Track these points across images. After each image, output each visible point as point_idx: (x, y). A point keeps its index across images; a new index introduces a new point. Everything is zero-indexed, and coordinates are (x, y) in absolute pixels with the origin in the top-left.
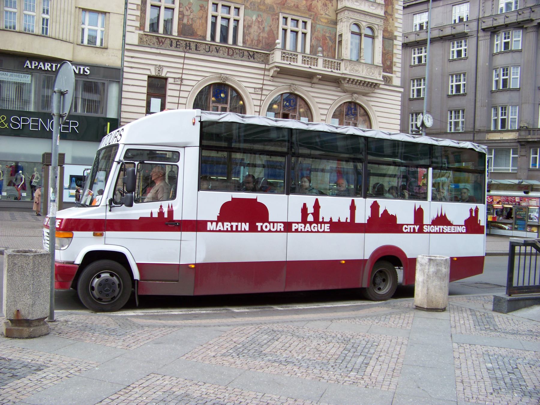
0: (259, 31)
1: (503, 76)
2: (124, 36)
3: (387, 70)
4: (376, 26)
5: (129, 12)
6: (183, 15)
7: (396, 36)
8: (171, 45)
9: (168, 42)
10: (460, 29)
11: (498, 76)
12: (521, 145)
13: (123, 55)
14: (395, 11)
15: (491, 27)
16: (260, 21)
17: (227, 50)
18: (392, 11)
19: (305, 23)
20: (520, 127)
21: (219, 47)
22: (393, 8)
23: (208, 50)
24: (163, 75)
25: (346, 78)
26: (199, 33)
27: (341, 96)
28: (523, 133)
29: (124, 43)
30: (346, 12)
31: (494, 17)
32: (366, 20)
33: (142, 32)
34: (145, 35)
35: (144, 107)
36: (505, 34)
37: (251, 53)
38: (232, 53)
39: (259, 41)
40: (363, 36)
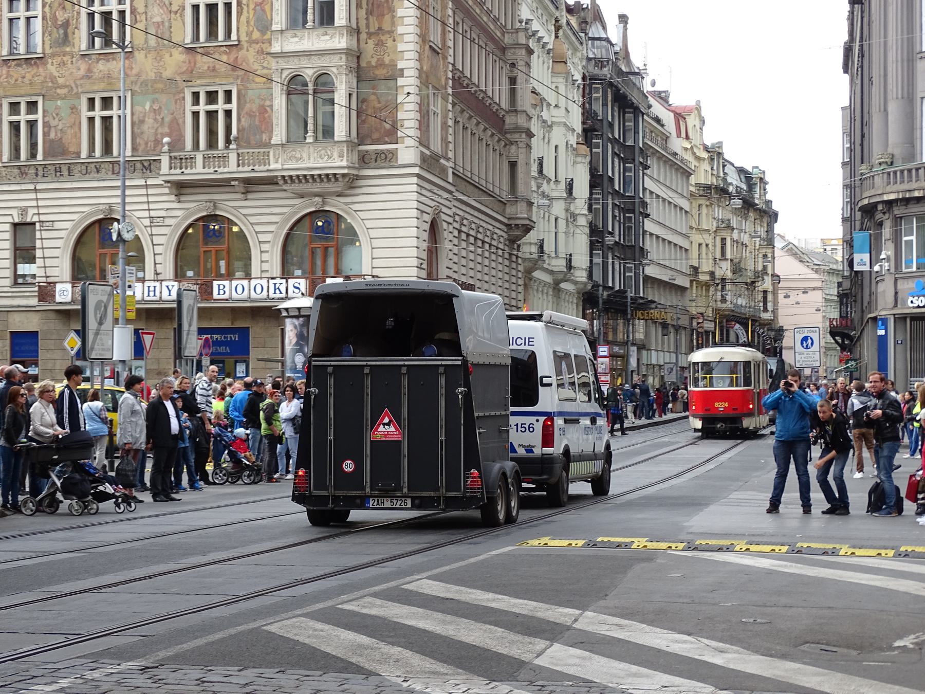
0: (156, 126)
3: (387, 139)
6: (50, 127)
7: (402, 70)
8: (37, 175)
16: (157, 108)
17: (111, 165)
18: (393, 24)
19: (228, 94)
22: (393, 17)
23: (84, 172)
24: (28, 220)
32: (311, 66)
34: (4, 167)
37: (146, 164)
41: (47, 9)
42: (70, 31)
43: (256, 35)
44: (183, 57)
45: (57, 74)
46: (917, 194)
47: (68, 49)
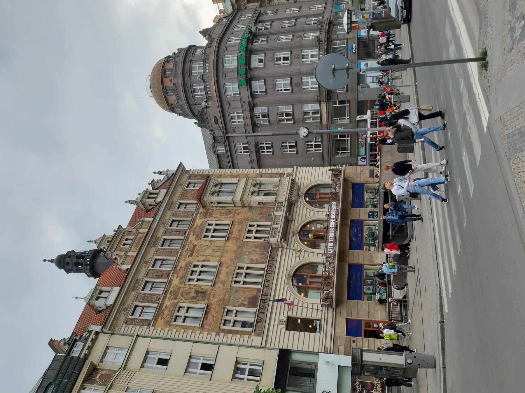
0: (255, 254)
1: (283, 116)
2: (255, 347)
4: (253, 182)
5: (237, 343)
6: (242, 304)
8: (264, 313)
9: (260, 315)
10: (253, 148)
11: (283, 120)
12: (330, 99)
13: (270, 348)
14: (243, 173)
15: (252, 127)
16: (248, 253)
17: (268, 275)
18: (243, 175)
19: (250, 226)
20: (318, 101)
21: (264, 286)
22: (241, 175)
23: (268, 287)
24: (286, 319)
25: (288, 198)
26: (255, 293)
27: (301, 203)
28: (322, 99)
29: (260, 347)
30: (244, 199)
31: (246, 125)
33: (253, 334)
34: (255, 331)
35: (310, 334)
36: (257, 118)
37: (271, 259)
38: (269, 271)
39: (262, 254)
40: (261, 189)
41: (186, 301)
42: (200, 290)
43: (231, 215)
44: (230, 241)
45: (217, 299)
46: (326, 48)
47: (209, 292)
